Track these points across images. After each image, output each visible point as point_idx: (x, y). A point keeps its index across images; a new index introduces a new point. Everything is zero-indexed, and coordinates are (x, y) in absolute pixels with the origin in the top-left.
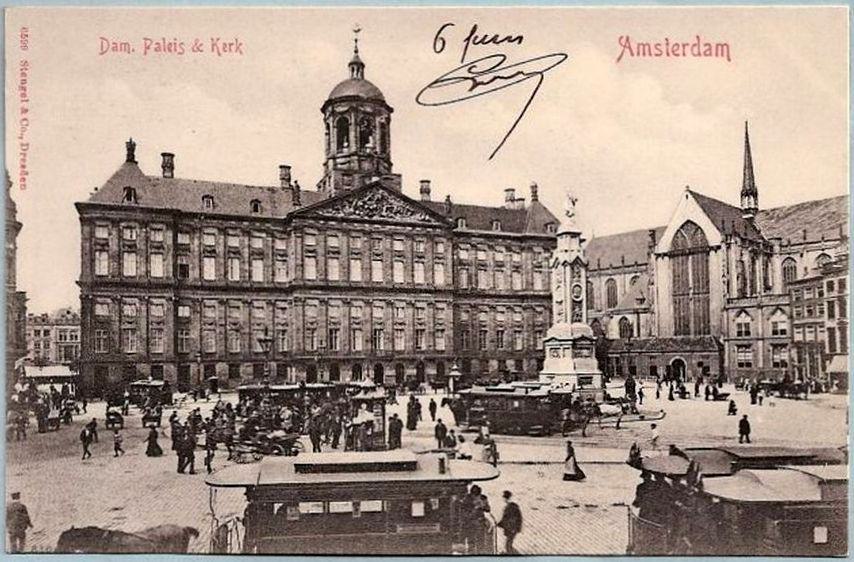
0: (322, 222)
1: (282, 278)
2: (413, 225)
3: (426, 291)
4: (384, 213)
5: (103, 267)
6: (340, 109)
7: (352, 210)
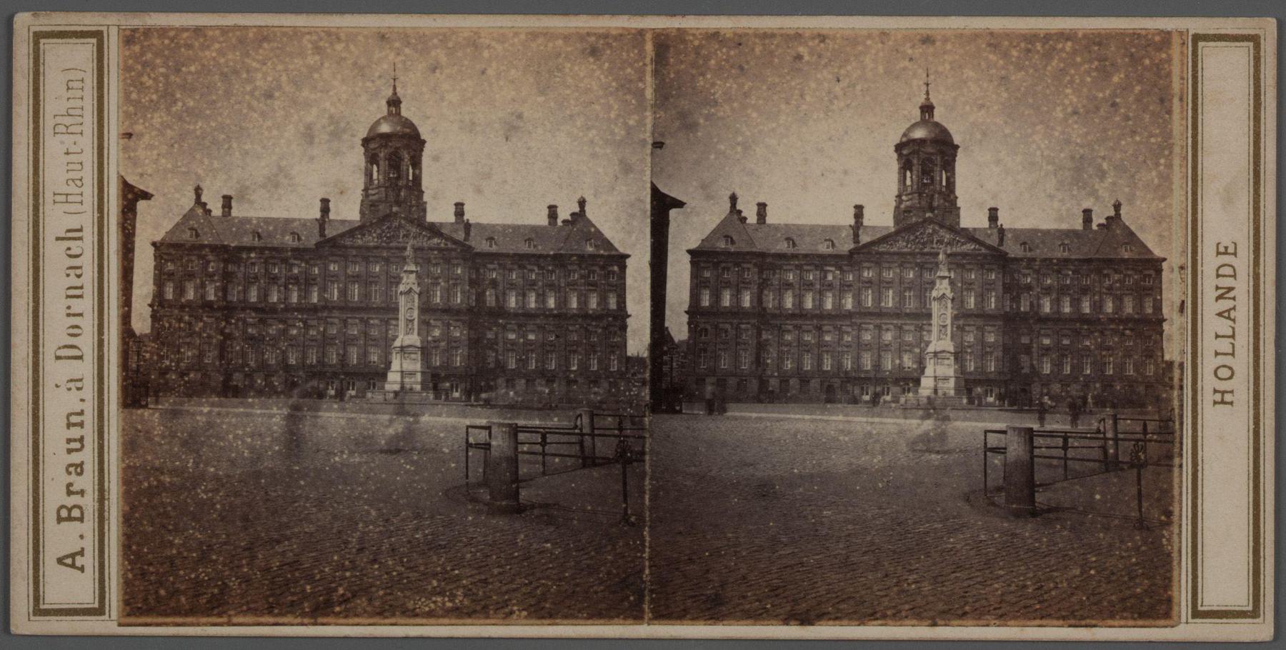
2: (964, 255)
3: (977, 316)
5: (706, 301)
6: (905, 152)
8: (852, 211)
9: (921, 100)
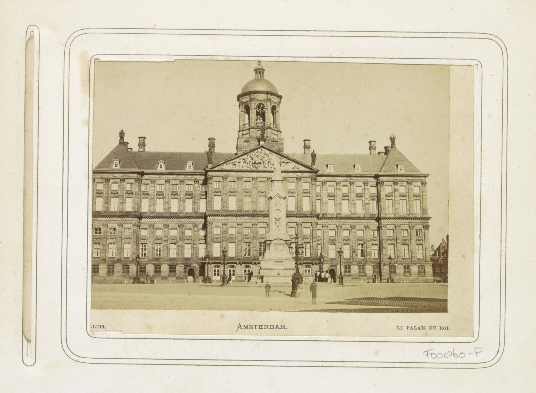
0: (225, 173)
1: (203, 209)
4: (267, 166)
5: (100, 207)
7: (245, 164)
8: (207, 142)
9: (255, 66)
